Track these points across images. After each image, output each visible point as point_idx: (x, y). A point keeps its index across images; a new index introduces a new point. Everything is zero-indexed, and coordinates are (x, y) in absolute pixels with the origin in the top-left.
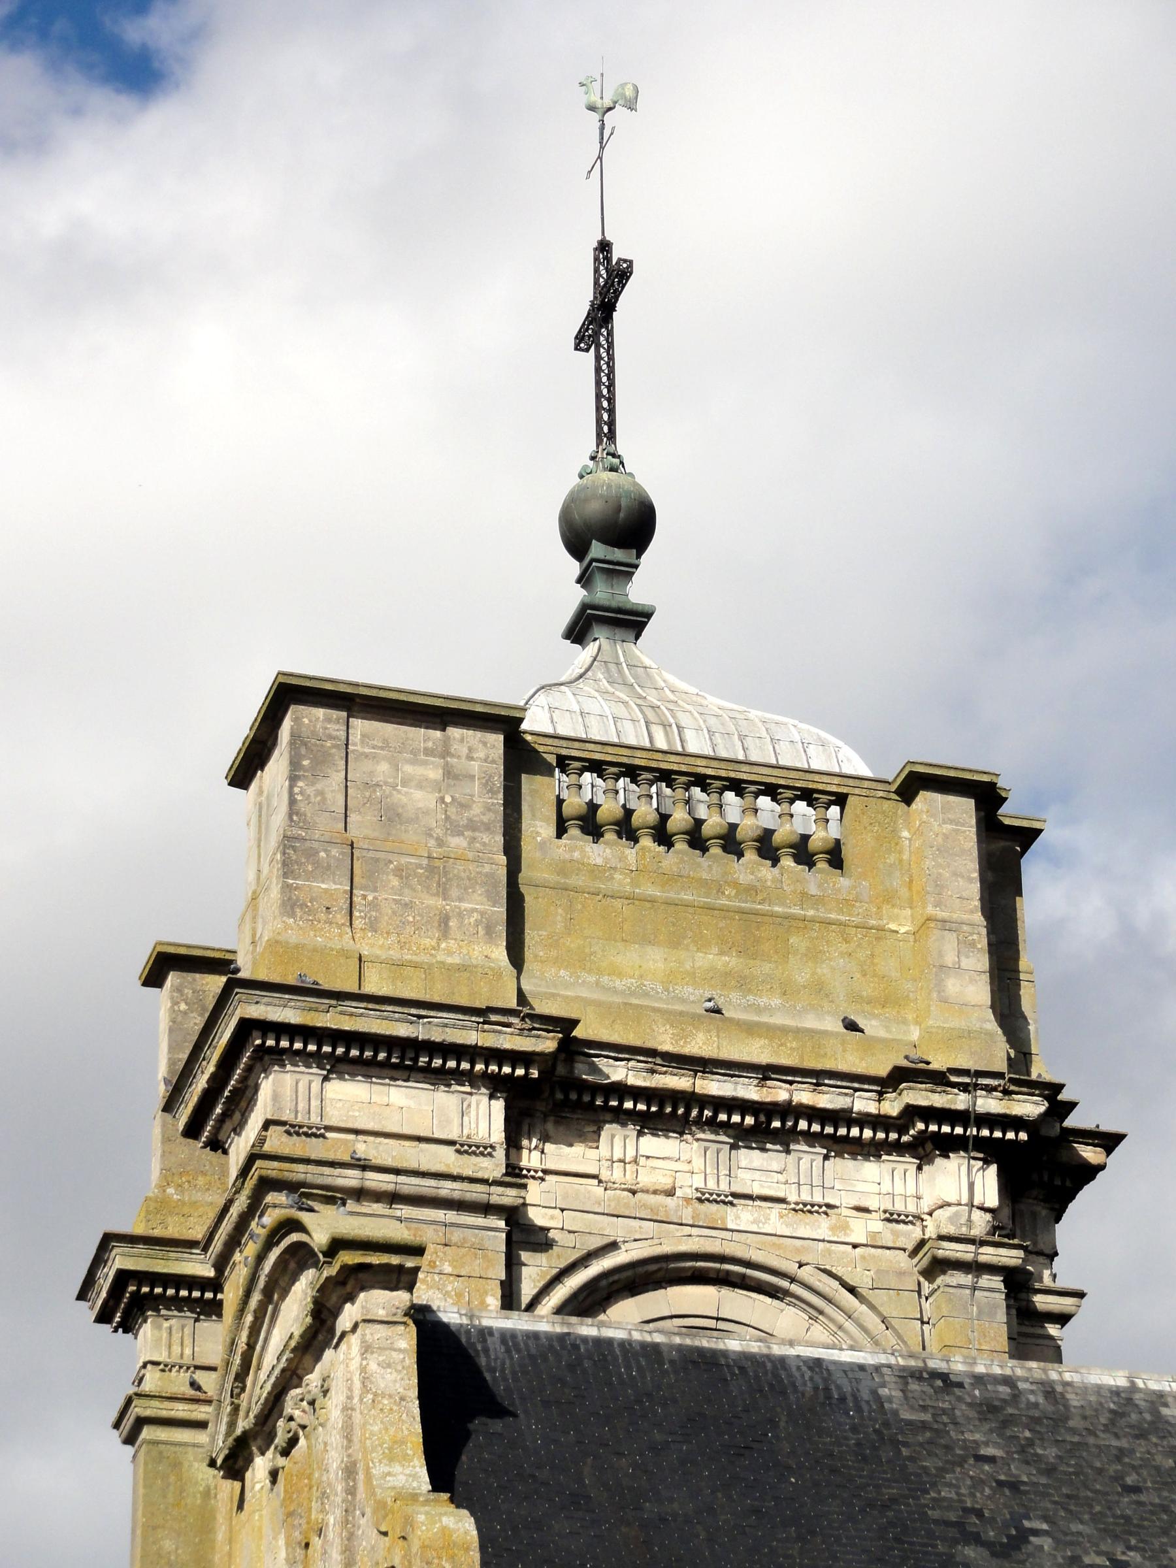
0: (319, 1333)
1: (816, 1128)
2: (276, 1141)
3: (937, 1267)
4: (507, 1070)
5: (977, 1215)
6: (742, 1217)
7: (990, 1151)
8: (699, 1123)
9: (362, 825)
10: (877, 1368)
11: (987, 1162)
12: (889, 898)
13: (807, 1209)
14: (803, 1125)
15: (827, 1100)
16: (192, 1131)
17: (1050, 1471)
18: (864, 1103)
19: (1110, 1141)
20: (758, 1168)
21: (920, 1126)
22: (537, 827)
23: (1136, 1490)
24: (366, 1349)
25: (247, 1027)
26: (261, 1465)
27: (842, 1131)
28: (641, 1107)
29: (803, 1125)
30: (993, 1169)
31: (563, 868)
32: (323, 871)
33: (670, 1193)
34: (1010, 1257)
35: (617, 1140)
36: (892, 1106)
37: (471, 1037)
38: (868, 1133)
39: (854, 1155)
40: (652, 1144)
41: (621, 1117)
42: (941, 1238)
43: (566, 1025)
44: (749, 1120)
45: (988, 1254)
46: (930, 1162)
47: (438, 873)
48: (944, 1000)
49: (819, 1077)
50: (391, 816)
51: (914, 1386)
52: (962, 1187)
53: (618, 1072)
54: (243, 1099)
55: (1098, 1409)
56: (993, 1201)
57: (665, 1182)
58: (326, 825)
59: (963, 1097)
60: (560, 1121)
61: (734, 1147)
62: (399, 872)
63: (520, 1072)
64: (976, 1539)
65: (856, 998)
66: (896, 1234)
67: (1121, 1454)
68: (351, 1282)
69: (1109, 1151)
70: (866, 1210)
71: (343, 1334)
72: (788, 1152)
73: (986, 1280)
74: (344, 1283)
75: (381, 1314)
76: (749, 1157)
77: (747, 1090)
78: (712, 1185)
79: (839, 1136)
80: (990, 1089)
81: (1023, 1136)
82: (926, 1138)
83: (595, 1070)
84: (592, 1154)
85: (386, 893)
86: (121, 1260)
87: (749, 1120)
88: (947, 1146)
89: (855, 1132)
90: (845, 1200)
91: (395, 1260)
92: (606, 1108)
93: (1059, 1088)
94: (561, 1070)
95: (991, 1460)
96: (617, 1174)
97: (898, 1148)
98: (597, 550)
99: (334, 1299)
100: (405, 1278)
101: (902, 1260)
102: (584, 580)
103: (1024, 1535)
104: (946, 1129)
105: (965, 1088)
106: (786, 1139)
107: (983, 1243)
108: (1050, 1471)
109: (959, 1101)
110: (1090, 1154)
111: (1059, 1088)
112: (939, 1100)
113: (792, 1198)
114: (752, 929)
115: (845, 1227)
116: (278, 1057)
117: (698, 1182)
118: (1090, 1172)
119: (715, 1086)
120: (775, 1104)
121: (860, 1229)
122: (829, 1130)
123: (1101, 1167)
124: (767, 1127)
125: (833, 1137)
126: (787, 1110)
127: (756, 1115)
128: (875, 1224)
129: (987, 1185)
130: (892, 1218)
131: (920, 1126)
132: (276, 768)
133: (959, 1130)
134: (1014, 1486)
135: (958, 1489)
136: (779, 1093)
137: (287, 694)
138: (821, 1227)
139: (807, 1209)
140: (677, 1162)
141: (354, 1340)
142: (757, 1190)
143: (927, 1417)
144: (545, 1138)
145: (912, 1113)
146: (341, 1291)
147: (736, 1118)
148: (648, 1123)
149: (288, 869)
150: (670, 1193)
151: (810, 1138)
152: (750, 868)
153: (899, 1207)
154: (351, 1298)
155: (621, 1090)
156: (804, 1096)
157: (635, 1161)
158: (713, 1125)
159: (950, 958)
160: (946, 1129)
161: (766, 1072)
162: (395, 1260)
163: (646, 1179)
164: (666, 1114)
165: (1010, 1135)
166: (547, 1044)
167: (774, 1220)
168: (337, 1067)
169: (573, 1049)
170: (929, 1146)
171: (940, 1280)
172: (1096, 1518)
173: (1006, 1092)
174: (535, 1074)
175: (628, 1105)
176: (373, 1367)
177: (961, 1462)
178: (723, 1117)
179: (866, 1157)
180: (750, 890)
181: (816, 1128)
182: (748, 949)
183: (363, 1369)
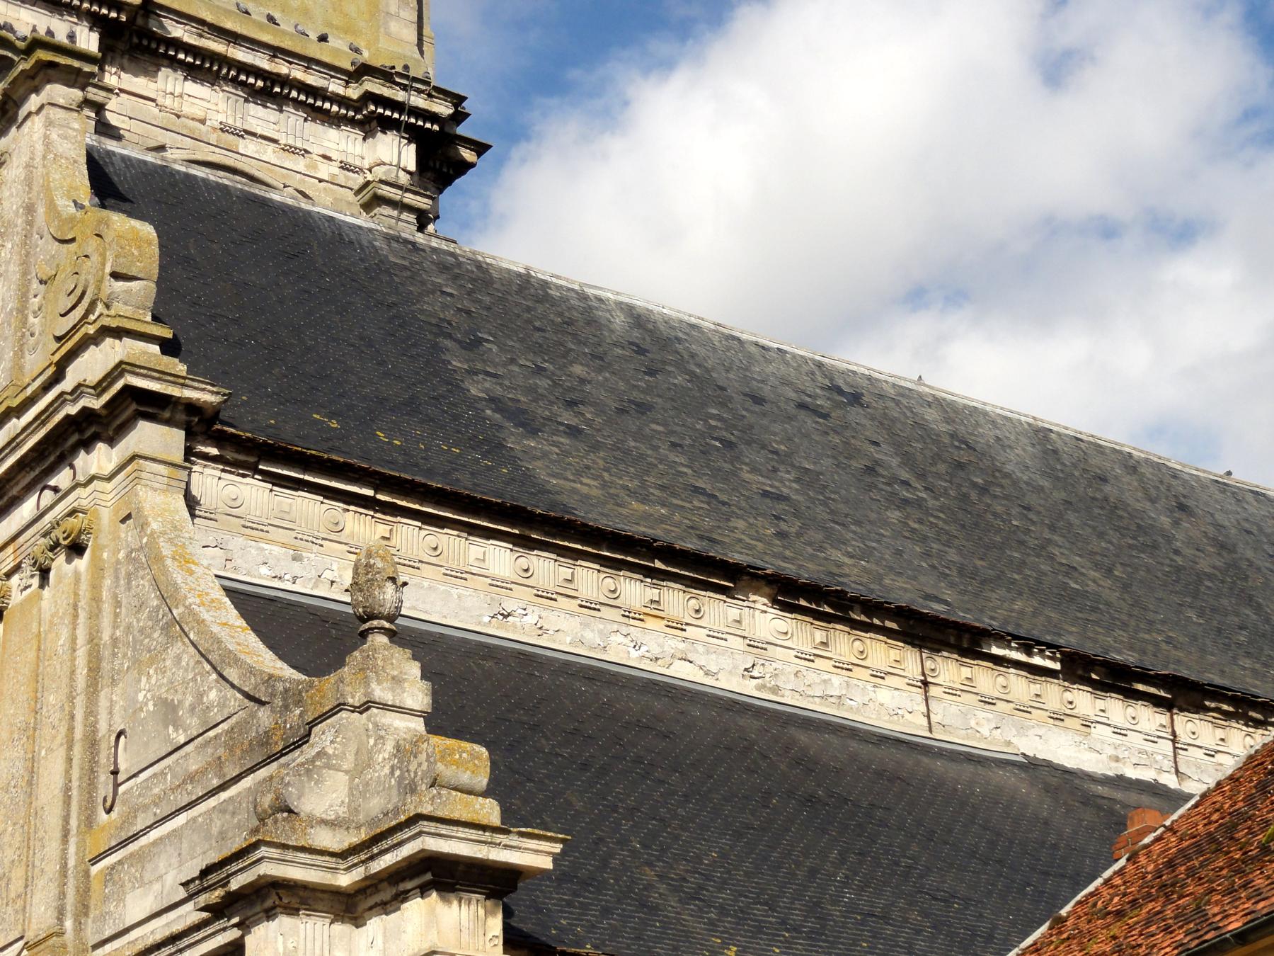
1: (302, 97)
3: (378, 200)
4: (104, 11)
5: (402, 173)
6: (249, 146)
7: (414, 135)
8: (225, 78)
10: (370, 230)
11: (410, 142)
14: (294, 94)
15: (313, 79)
17: (489, 309)
18: (335, 87)
19: (481, 149)
20: (260, 117)
21: (372, 108)
23: (539, 330)
24: (49, 124)
27: (319, 103)
28: (190, 59)
29: (294, 94)
30: (413, 147)
33: (203, 122)
34: (422, 202)
35: (168, 83)
36: (354, 92)
38: (335, 108)
39: (323, 122)
40: (192, 87)
41: (174, 64)
42: (381, 181)
44: (260, 83)
45: (410, 199)
46: (373, 136)
48: (388, 34)
49: (310, 62)
51: (395, 245)
52: (394, 154)
53: (177, 31)
55: (510, 282)
56: (412, 167)
57: (200, 114)
59: (402, 93)
60: (133, 59)
61: (246, 100)
63: (114, 15)
64: (450, 336)
65: (330, 25)
66: (347, 178)
67: (529, 309)
68: (47, 72)
69: (479, 156)
70: (329, 159)
71: (29, 114)
72: (281, 111)
73: (405, 216)
74: (33, 78)
75: (61, 102)
76: (255, 110)
78: (230, 121)
79: (316, 105)
80: (419, 91)
81: (436, 127)
82: (371, 118)
83: (162, 26)
84: (152, 85)
87: (260, 83)
88: (387, 125)
89: (327, 105)
91: (76, 64)
92: (166, 56)
93: (463, 99)
94: (140, 21)
95: (451, 295)
96: (168, 101)
97: (352, 122)
99: (21, 91)
100: (81, 80)
101: (350, 194)
103: (479, 342)
104: (388, 113)
105: (404, 88)
106: (280, 101)
107: (407, 190)
108: (489, 309)
109: (400, 96)
110: (468, 155)
111: (463, 99)
113: (283, 141)
115: (315, 167)
117: (221, 118)
118: (466, 166)
119: (241, 54)
120: (278, 75)
121: (325, 170)
122: (311, 101)
123: (472, 165)
124: (270, 90)
125: (312, 106)
126: (285, 81)
127: (264, 80)
128: (334, 169)
129: (410, 156)
130: (345, 167)
131: (372, 108)
133: (396, 115)
134: (468, 312)
135: (431, 306)
136: (282, 68)
138: (300, 164)
140: (211, 103)
141: (37, 123)
142: (259, 131)
143: (406, 263)
144: (123, 69)
145: (369, 97)
146: (30, 83)
147: (251, 80)
148: (192, 72)
150: (203, 122)
151: (298, 104)
153: (350, 160)
154: (37, 90)
155: (178, 44)
156: (298, 73)
157: (181, 96)
158: (235, 82)
159: (393, 9)
160: (388, 113)
161: (276, 52)
162: (76, 64)
163: (187, 109)
164: (205, 68)
165: (428, 125)
167: (269, 153)
170: (374, 123)
171: (377, 210)
172: (521, 341)
173: (430, 95)
174: (124, 18)
175: (181, 56)
176: (54, 136)
177: (433, 292)
178: (243, 77)
179: (331, 125)
181: (302, 97)
183: (46, 137)
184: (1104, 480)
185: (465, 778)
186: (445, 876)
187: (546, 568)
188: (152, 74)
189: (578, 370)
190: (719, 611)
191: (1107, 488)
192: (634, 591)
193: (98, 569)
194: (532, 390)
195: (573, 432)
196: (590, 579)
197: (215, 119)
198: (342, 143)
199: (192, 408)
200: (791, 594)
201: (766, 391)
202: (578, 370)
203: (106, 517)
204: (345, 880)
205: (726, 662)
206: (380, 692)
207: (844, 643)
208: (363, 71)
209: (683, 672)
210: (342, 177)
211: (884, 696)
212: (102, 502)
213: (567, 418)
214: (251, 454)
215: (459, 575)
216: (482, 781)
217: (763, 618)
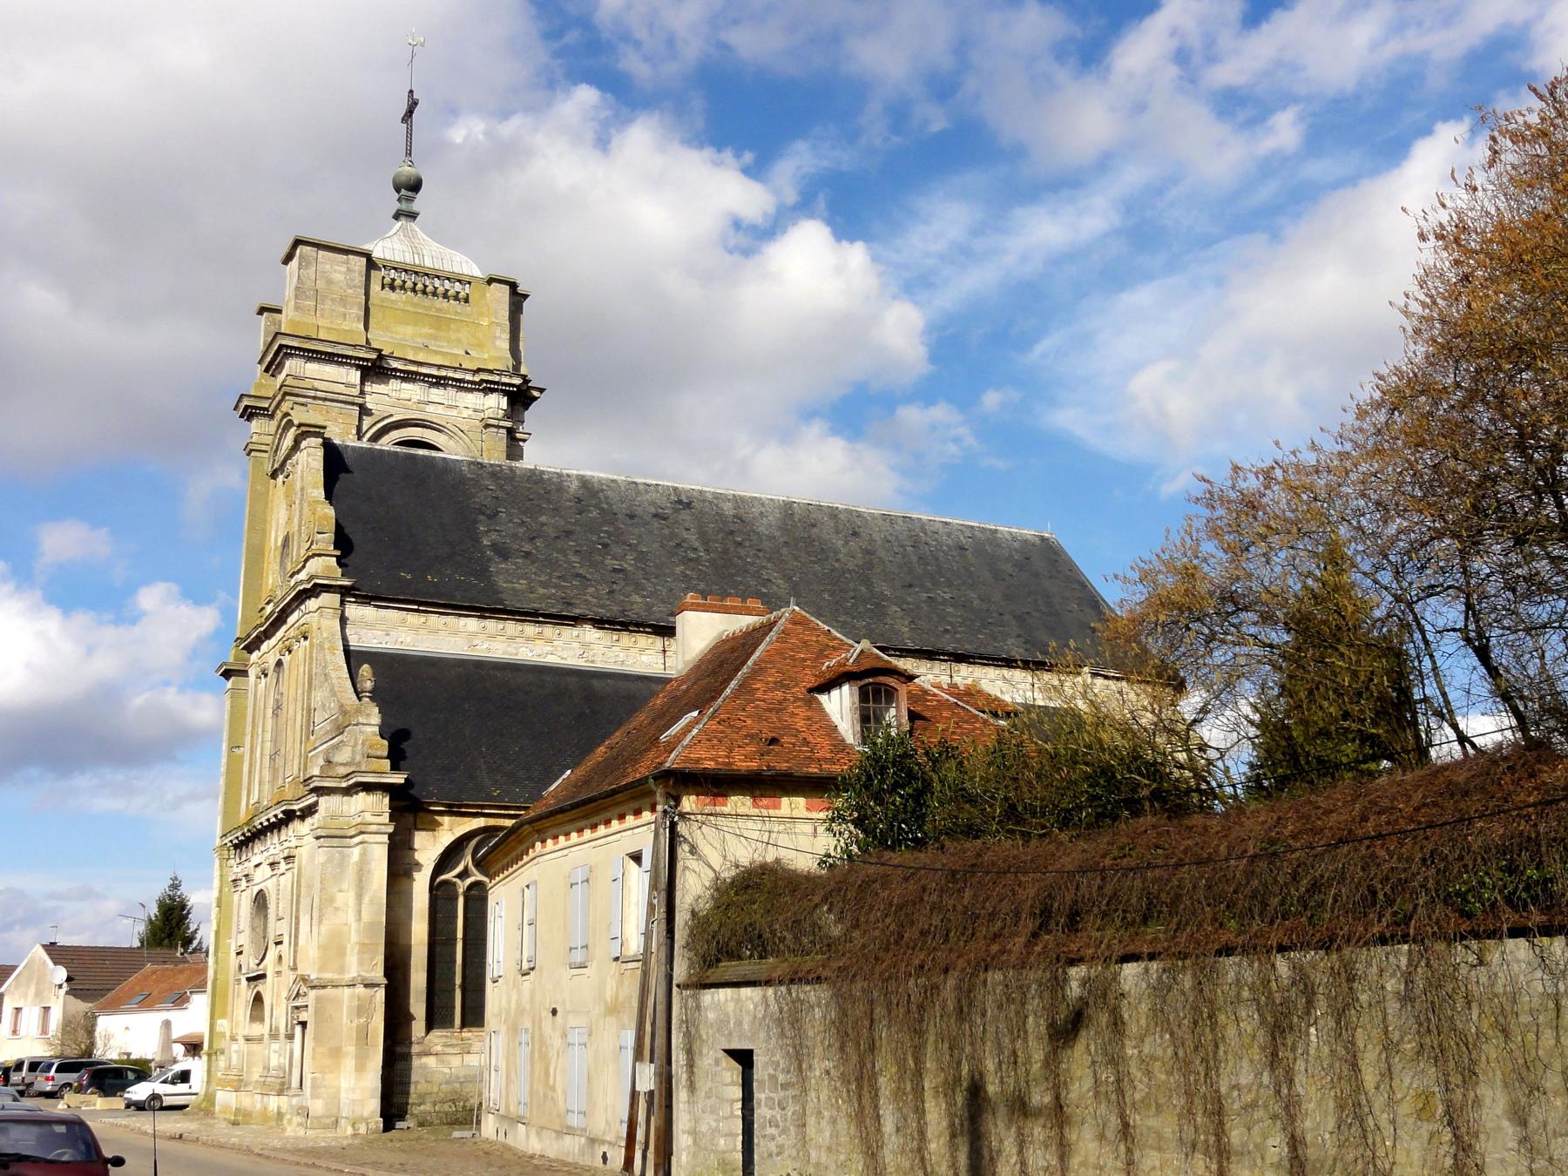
0: (296, 447)
2: (290, 381)
3: (487, 426)
6: (431, 408)
7: (505, 393)
9: (320, 284)
12: (481, 314)
13: (450, 407)
15: (457, 376)
16: (267, 370)
18: (469, 377)
19: (542, 390)
20: (437, 394)
22: (375, 287)
25: (281, 347)
26: (281, 478)
31: (383, 300)
32: (308, 298)
34: (509, 424)
35: (394, 384)
36: (477, 378)
37: (351, 353)
40: (405, 385)
41: (396, 377)
43: (379, 351)
47: (343, 301)
50: (330, 282)
52: (496, 404)
53: (395, 364)
54: (281, 366)
58: (309, 284)
62: (332, 300)
76: (434, 390)
77: (434, 372)
79: (460, 385)
82: (488, 388)
85: (328, 305)
86: (246, 402)
88: (492, 391)
90: (462, 405)
98: (403, 192)
102: (399, 200)
106: (445, 386)
109: (497, 378)
110: (536, 394)
112: (490, 378)
114: (439, 322)
116: (291, 355)
118: (536, 399)
121: (466, 413)
124: (439, 382)
126: (445, 378)
128: (470, 412)
129: (504, 402)
132: (295, 262)
135: (481, 498)
136: (443, 373)
137: (298, 242)
138: (454, 412)
139: (450, 407)
140: (413, 391)
145: (482, 381)
148: (404, 379)
149: (296, 297)
152: (440, 302)
155: (396, 370)
156: (451, 374)
161: (440, 367)
164: (409, 377)
166: (374, 356)
167: (440, 410)
168: (309, 359)
169: (381, 357)
180: (439, 310)
182: (438, 328)
184: (814, 526)
185: (379, 753)
186: (368, 788)
187: (491, 625)
188: (387, 383)
189: (543, 519)
190: (569, 633)
191: (815, 530)
192: (530, 629)
193: (312, 645)
194: (515, 535)
195: (527, 554)
196: (511, 627)
197: (415, 398)
198: (473, 399)
199: (341, 587)
200: (599, 623)
201: (639, 511)
202: (543, 519)
203: (315, 626)
204: (344, 785)
205: (571, 653)
206: (361, 720)
207: (626, 639)
208: (479, 370)
209: (552, 660)
210: (474, 415)
211: (644, 658)
212: (313, 619)
213: (527, 547)
214: (366, 600)
215: (456, 633)
216: (386, 754)
217: (590, 633)
